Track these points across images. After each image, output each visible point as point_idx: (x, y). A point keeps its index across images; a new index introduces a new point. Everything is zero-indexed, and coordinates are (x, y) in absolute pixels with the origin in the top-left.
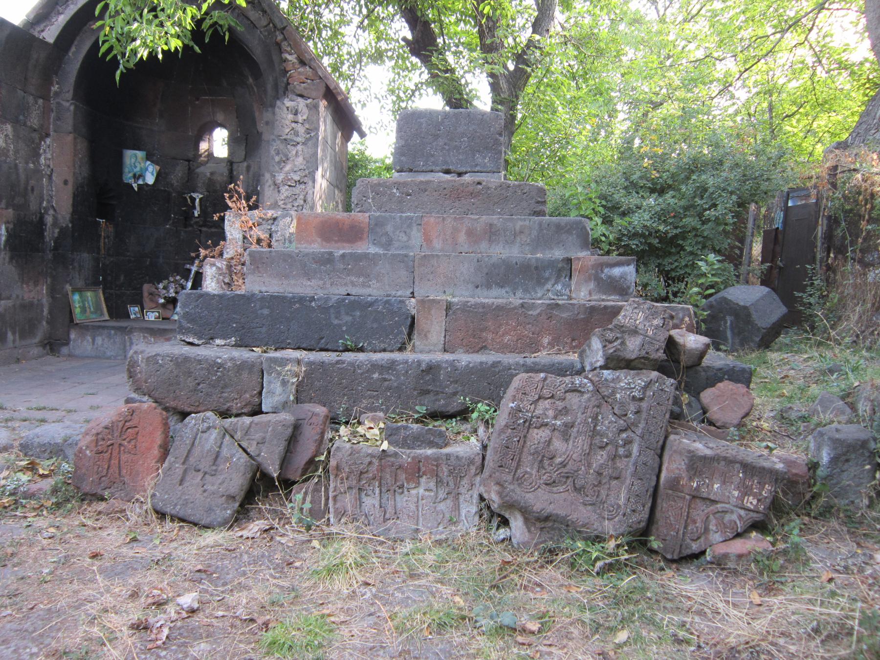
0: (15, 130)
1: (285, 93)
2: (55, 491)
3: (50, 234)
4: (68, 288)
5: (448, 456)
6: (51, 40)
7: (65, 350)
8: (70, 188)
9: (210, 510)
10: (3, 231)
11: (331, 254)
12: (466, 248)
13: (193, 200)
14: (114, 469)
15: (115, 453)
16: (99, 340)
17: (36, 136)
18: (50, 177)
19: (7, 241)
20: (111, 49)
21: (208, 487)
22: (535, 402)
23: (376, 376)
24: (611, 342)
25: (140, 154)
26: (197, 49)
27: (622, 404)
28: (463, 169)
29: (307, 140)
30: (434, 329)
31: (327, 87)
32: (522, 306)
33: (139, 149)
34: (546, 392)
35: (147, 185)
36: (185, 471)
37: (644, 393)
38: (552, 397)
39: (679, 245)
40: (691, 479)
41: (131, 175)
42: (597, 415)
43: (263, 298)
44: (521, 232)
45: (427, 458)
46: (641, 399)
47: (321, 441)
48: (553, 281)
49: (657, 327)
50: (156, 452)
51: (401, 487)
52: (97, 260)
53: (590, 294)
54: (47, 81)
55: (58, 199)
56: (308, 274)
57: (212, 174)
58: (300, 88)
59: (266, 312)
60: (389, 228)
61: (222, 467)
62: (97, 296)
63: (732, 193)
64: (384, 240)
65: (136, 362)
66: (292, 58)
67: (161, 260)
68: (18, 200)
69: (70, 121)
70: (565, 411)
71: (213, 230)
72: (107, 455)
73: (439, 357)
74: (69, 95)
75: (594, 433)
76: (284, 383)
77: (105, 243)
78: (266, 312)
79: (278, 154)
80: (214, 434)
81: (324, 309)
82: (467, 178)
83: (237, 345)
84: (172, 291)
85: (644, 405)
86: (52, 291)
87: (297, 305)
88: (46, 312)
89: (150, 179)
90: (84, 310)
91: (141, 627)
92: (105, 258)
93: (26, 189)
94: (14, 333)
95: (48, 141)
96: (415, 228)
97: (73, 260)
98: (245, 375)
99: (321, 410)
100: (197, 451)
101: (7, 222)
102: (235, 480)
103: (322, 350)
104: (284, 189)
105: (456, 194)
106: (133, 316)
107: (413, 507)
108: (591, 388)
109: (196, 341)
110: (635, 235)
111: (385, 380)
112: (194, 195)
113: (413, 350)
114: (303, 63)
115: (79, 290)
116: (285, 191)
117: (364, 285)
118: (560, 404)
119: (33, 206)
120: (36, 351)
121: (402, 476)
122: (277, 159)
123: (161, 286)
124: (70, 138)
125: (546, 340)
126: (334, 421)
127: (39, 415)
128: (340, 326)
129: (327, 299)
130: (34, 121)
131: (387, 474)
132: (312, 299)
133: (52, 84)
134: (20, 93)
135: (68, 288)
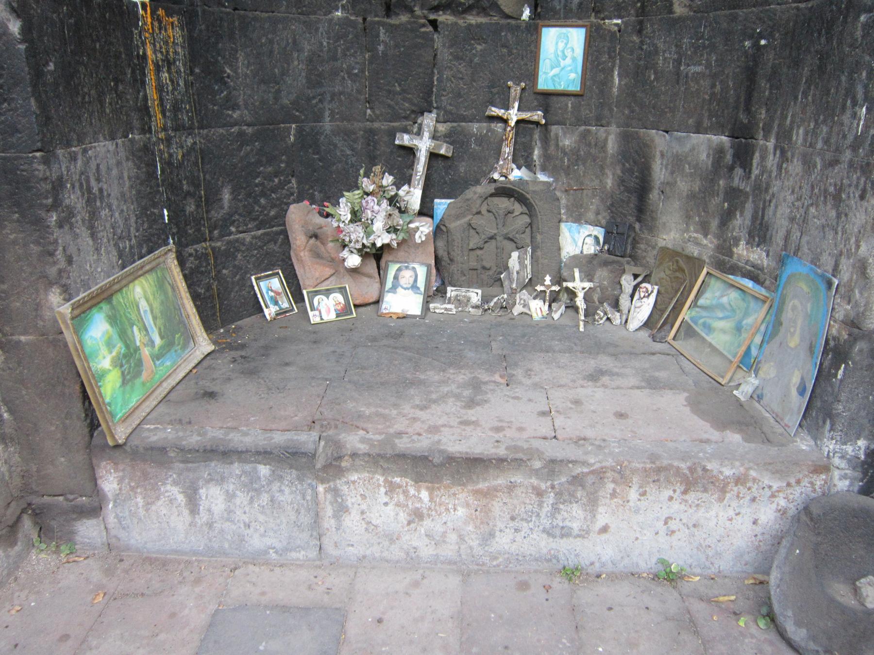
7: (88, 531)
16: (213, 498)
52: (144, 155)
67: (327, 125)
71: (473, 19)
77: (160, 88)
84: (378, 225)
92: (168, 141)
97: (58, 185)
106: (270, 312)
123: (344, 211)
135: (58, 305)
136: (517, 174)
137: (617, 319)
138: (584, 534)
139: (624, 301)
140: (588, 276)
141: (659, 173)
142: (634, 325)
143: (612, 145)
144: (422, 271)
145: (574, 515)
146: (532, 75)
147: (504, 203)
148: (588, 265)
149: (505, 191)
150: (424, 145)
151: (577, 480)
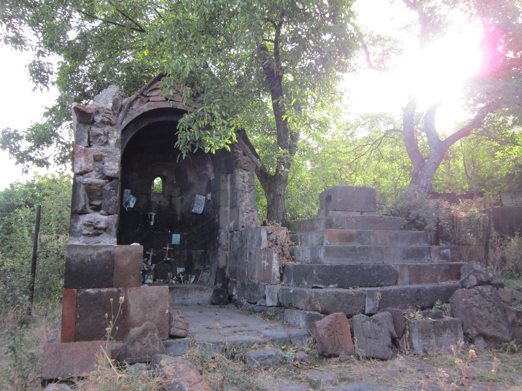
11: (355, 247)
13: (151, 216)
15: (335, 335)
25: (129, 191)
35: (130, 208)
40: (518, 319)
41: (125, 203)
43: (347, 266)
51: (441, 334)
57: (160, 202)
58: (245, 166)
59: (348, 272)
61: (379, 335)
65: (312, 297)
66: (241, 152)
72: (332, 336)
78: (348, 272)
79: (241, 197)
81: (369, 270)
82: (365, 214)
83: (338, 287)
87: (359, 269)
89: (132, 205)
98: (360, 298)
109: (322, 287)
111: (406, 296)
114: (244, 154)
117: (367, 260)
122: (240, 200)
125: (439, 278)
128: (374, 276)
136: (168, 259)
137: (188, 282)
138: (187, 299)
139: (189, 279)
140: (182, 275)
141: (194, 257)
142: (191, 282)
143: (186, 253)
144: (152, 276)
145: (186, 296)
146: (171, 241)
147: (166, 264)
148: (182, 273)
149: (167, 262)
150: (151, 254)
151: (186, 290)
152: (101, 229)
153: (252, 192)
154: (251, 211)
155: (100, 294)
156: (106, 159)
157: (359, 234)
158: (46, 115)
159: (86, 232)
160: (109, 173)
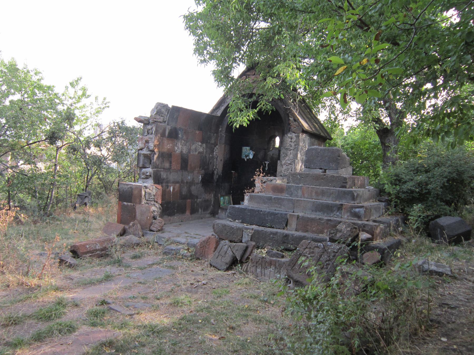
0: (206, 145)
1: (289, 131)
2: (191, 256)
3: (216, 177)
4: (219, 195)
5: (279, 261)
6: (219, 115)
7: (217, 216)
8: (222, 162)
9: (221, 266)
10: (200, 177)
12: (315, 197)
13: (265, 164)
14: (204, 252)
17: (213, 146)
18: (217, 158)
19: (201, 180)
20: (231, 122)
21: (222, 260)
22: (305, 249)
23: (271, 236)
24: (332, 234)
25: (248, 148)
26: (259, 118)
27: (330, 253)
28: (326, 168)
29: (295, 148)
30: (293, 223)
31: (303, 129)
32: (320, 219)
33: (248, 146)
34: (309, 247)
36: (218, 255)
37: (338, 251)
38: (310, 248)
39: (427, 197)
42: (322, 255)
44: (332, 193)
45: (273, 260)
46: (337, 252)
47: (251, 252)
48: (336, 211)
49: (348, 231)
50: (213, 249)
53: (348, 217)
54: (218, 127)
55: (218, 166)
56: (265, 203)
57: (273, 154)
60: (292, 189)
62: (229, 198)
63: (446, 177)
64: (290, 193)
68: (206, 167)
69: (224, 140)
70: (313, 252)
73: (293, 232)
74: (224, 132)
75: (319, 260)
76: (248, 235)
78: (249, 214)
80: (227, 246)
85: (337, 254)
86: (215, 196)
88: (212, 202)
89: (251, 157)
90: (224, 203)
91: (192, 284)
93: (208, 164)
94: (201, 209)
95: (217, 147)
96: (299, 190)
98: (239, 232)
99: (254, 243)
100: (222, 250)
101: (202, 174)
102: (228, 259)
103: (263, 226)
104: (284, 166)
105: (317, 178)
107: (269, 273)
108: (322, 247)
110: (404, 193)
111: (274, 237)
112: (266, 162)
113: (287, 230)
115: (223, 196)
116: (285, 167)
117: (280, 207)
118: (312, 250)
119: (211, 169)
120: (208, 215)
121: (267, 264)
122: (283, 155)
124: (223, 146)
126: (258, 248)
127: (195, 236)
129: (265, 211)
130: (213, 141)
131: (263, 263)
132: (261, 211)
133: (219, 128)
134: (209, 133)
152: (148, 176)
153: (295, 150)
154: (290, 164)
155: (128, 205)
156: (150, 141)
157: (289, 187)
158: (139, 120)
159: (142, 177)
160: (151, 148)
